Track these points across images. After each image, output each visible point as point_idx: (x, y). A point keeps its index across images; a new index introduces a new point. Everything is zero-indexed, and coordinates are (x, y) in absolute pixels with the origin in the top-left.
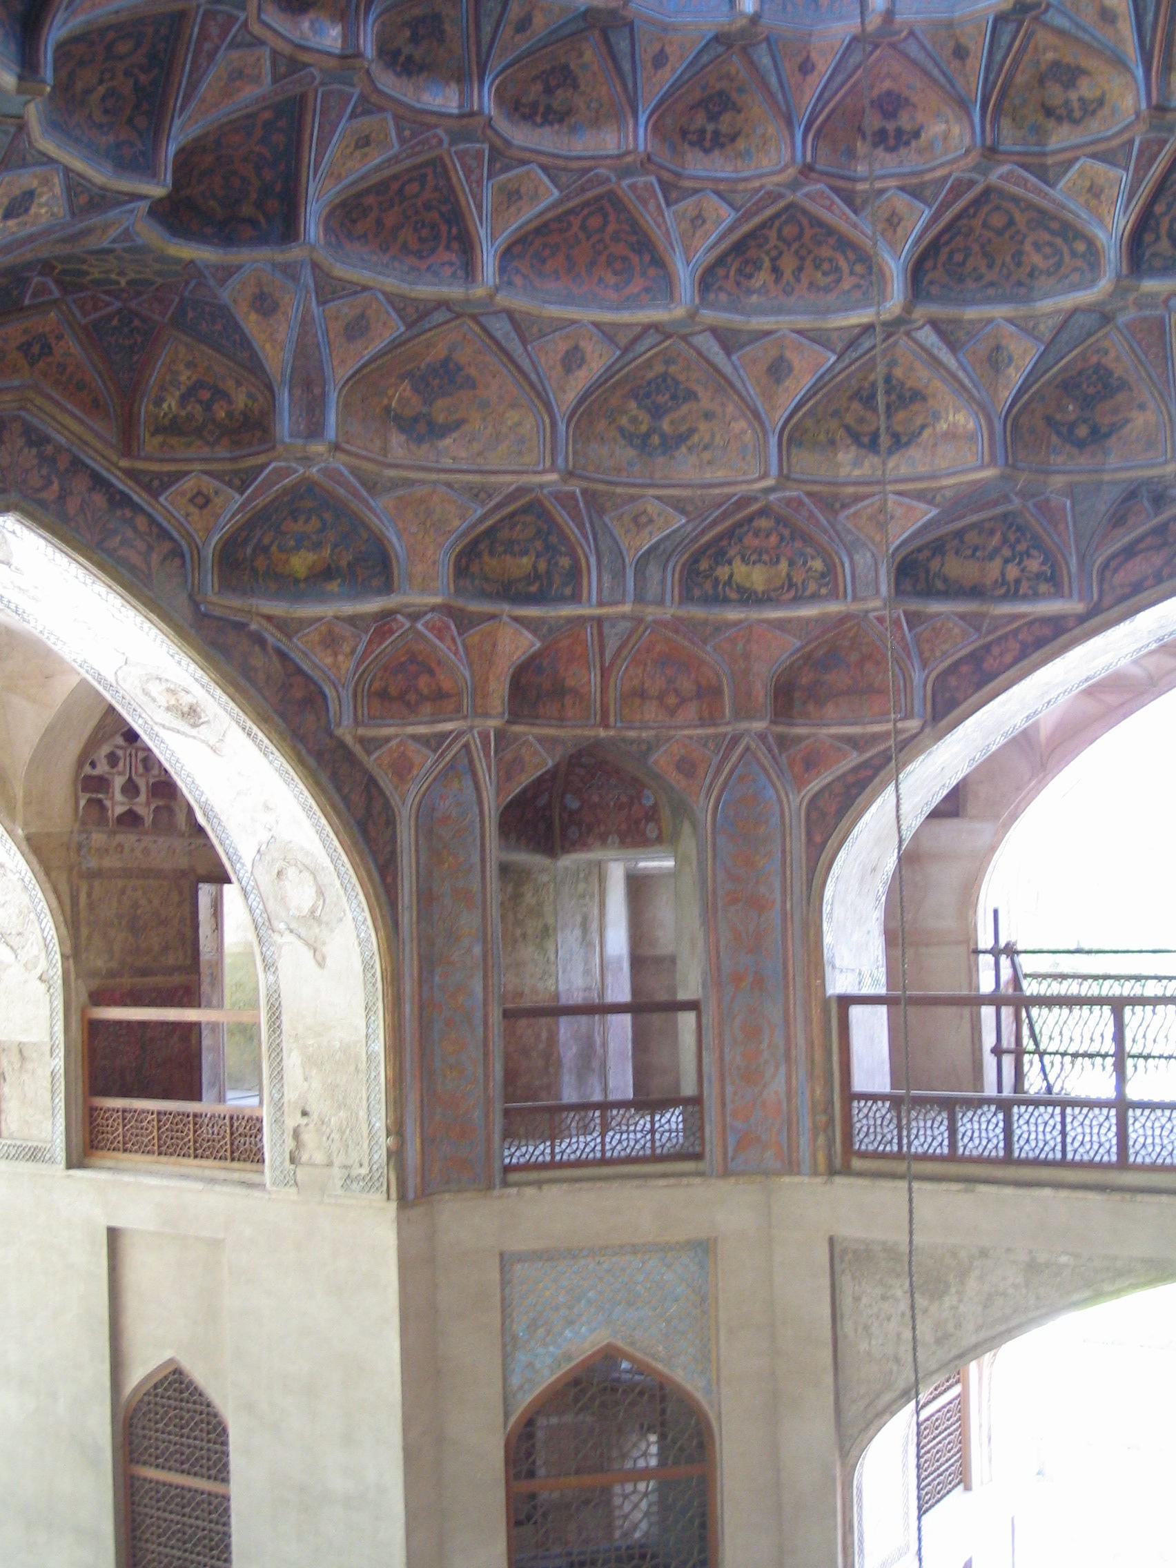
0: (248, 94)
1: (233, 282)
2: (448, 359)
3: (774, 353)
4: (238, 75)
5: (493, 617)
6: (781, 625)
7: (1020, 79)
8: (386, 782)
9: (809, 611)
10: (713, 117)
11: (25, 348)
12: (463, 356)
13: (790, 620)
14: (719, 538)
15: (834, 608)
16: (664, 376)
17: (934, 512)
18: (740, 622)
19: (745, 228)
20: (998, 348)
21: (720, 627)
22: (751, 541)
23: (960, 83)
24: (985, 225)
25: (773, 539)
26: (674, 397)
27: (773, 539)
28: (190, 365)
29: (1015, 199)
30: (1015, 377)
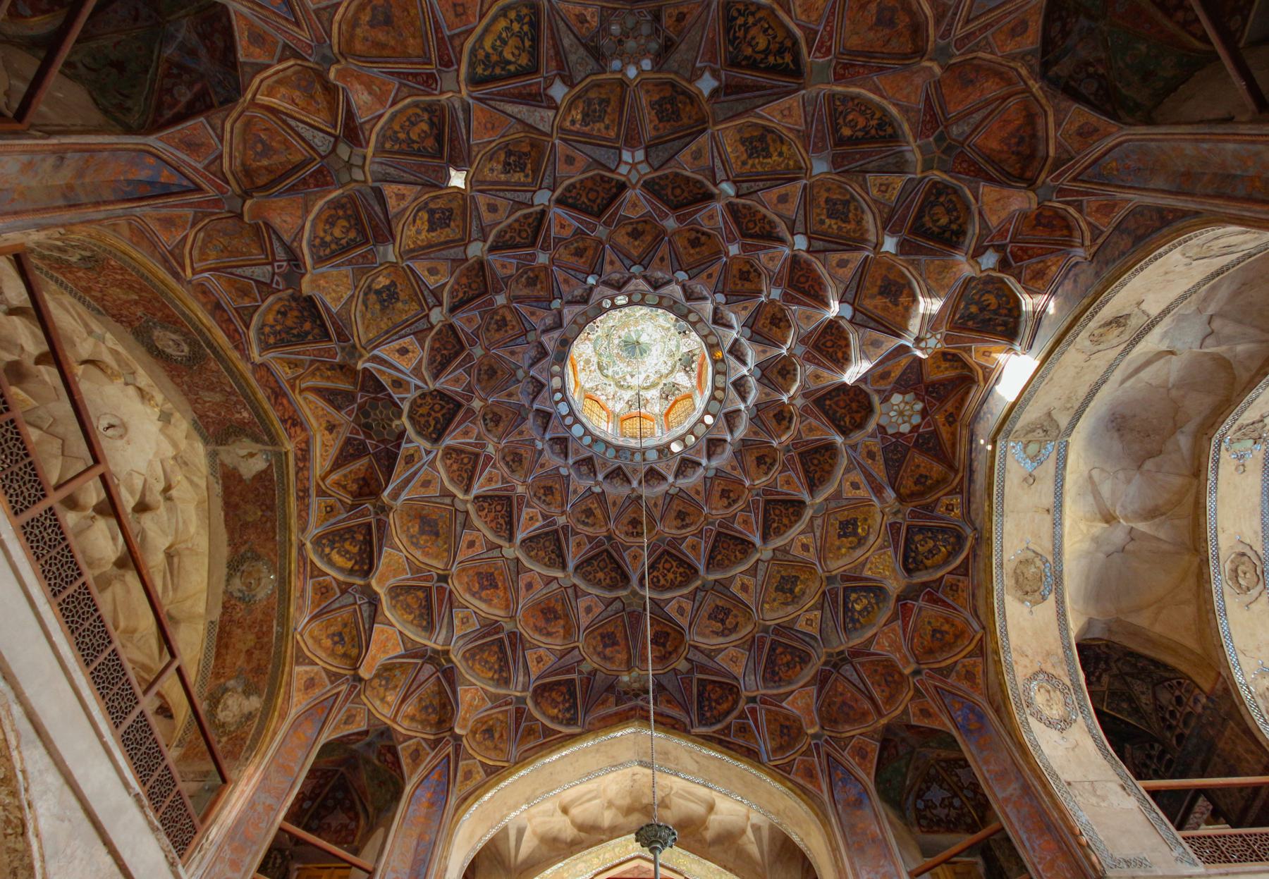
0: (815, 423)
1: (883, 388)
2: (881, 293)
3: (780, 206)
4: (811, 430)
5: (980, 214)
6: (877, 90)
7: (649, 238)
8: (1119, 215)
9: (854, 90)
10: (748, 272)
11: (950, 424)
12: (876, 290)
13: (870, 90)
14: (873, 140)
15: (839, 89)
16: (829, 217)
17: (757, 110)
18: (894, 105)
19: (762, 243)
20: (695, 159)
21: (905, 110)
22: (861, 122)
23: (667, 250)
24: (683, 191)
25: (850, 117)
26: (835, 204)
27: (850, 117)
28: (938, 367)
29: (666, 203)
30: (693, 146)
